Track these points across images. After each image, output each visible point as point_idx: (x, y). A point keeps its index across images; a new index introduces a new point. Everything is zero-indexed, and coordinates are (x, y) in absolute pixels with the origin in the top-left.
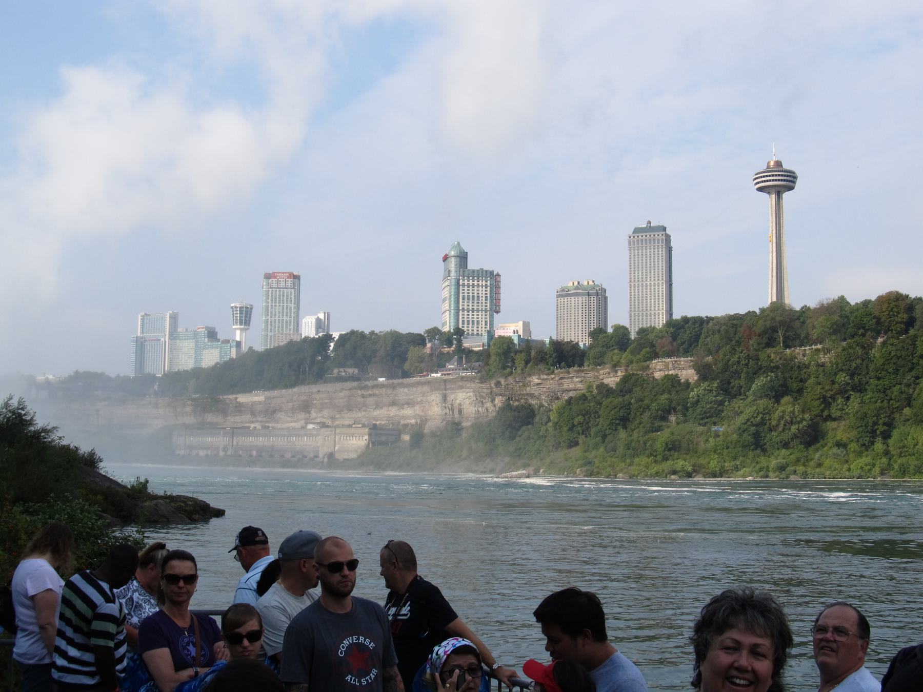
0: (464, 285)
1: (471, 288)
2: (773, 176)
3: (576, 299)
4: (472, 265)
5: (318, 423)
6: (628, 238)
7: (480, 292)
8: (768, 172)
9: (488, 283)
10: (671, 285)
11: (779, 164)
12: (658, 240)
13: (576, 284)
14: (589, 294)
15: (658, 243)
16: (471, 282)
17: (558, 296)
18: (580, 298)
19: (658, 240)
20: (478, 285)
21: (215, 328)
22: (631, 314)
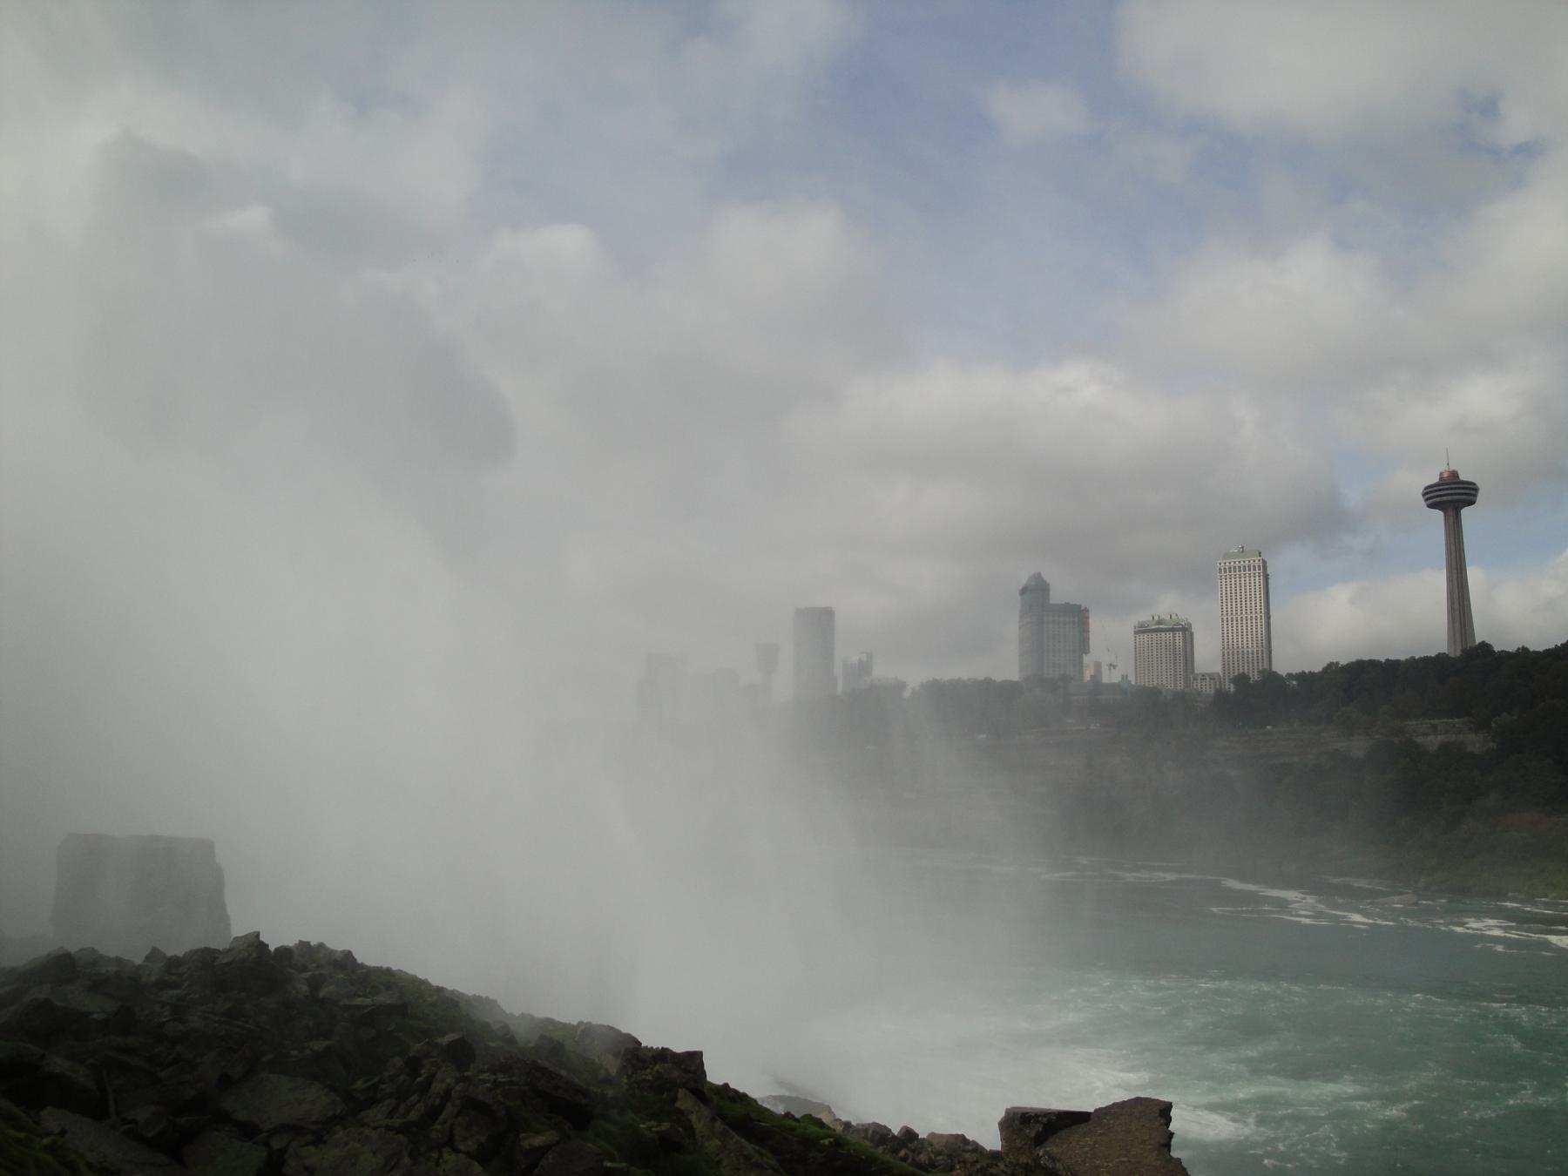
2: (1452, 489)
3: (1159, 636)
8: (1442, 485)
9: (1076, 619)
11: (1454, 474)
12: (1254, 566)
13: (1156, 618)
14: (1172, 630)
15: (1255, 570)
17: (1136, 633)
18: (1163, 634)
19: (1254, 566)
22: (1223, 653)
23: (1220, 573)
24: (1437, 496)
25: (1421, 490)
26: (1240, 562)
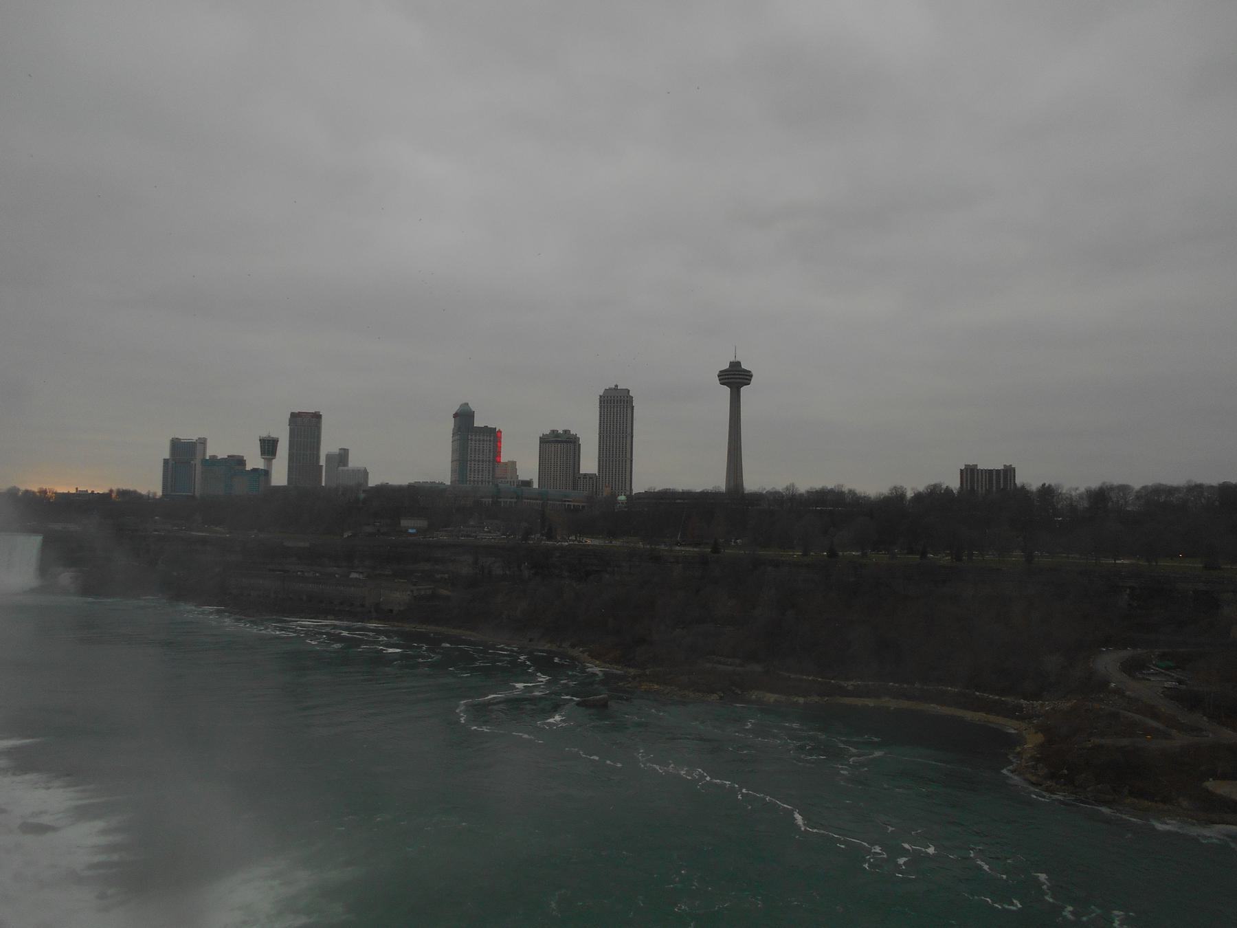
0: (471, 439)
1: (477, 443)
4: (479, 422)
5: (361, 573)
6: (599, 397)
7: (485, 446)
9: (492, 438)
10: (632, 437)
11: (738, 364)
14: (566, 442)
16: (478, 437)
20: (484, 440)
21: (243, 457)
23: (600, 403)
24: (726, 379)
25: (718, 373)
26: (614, 397)
